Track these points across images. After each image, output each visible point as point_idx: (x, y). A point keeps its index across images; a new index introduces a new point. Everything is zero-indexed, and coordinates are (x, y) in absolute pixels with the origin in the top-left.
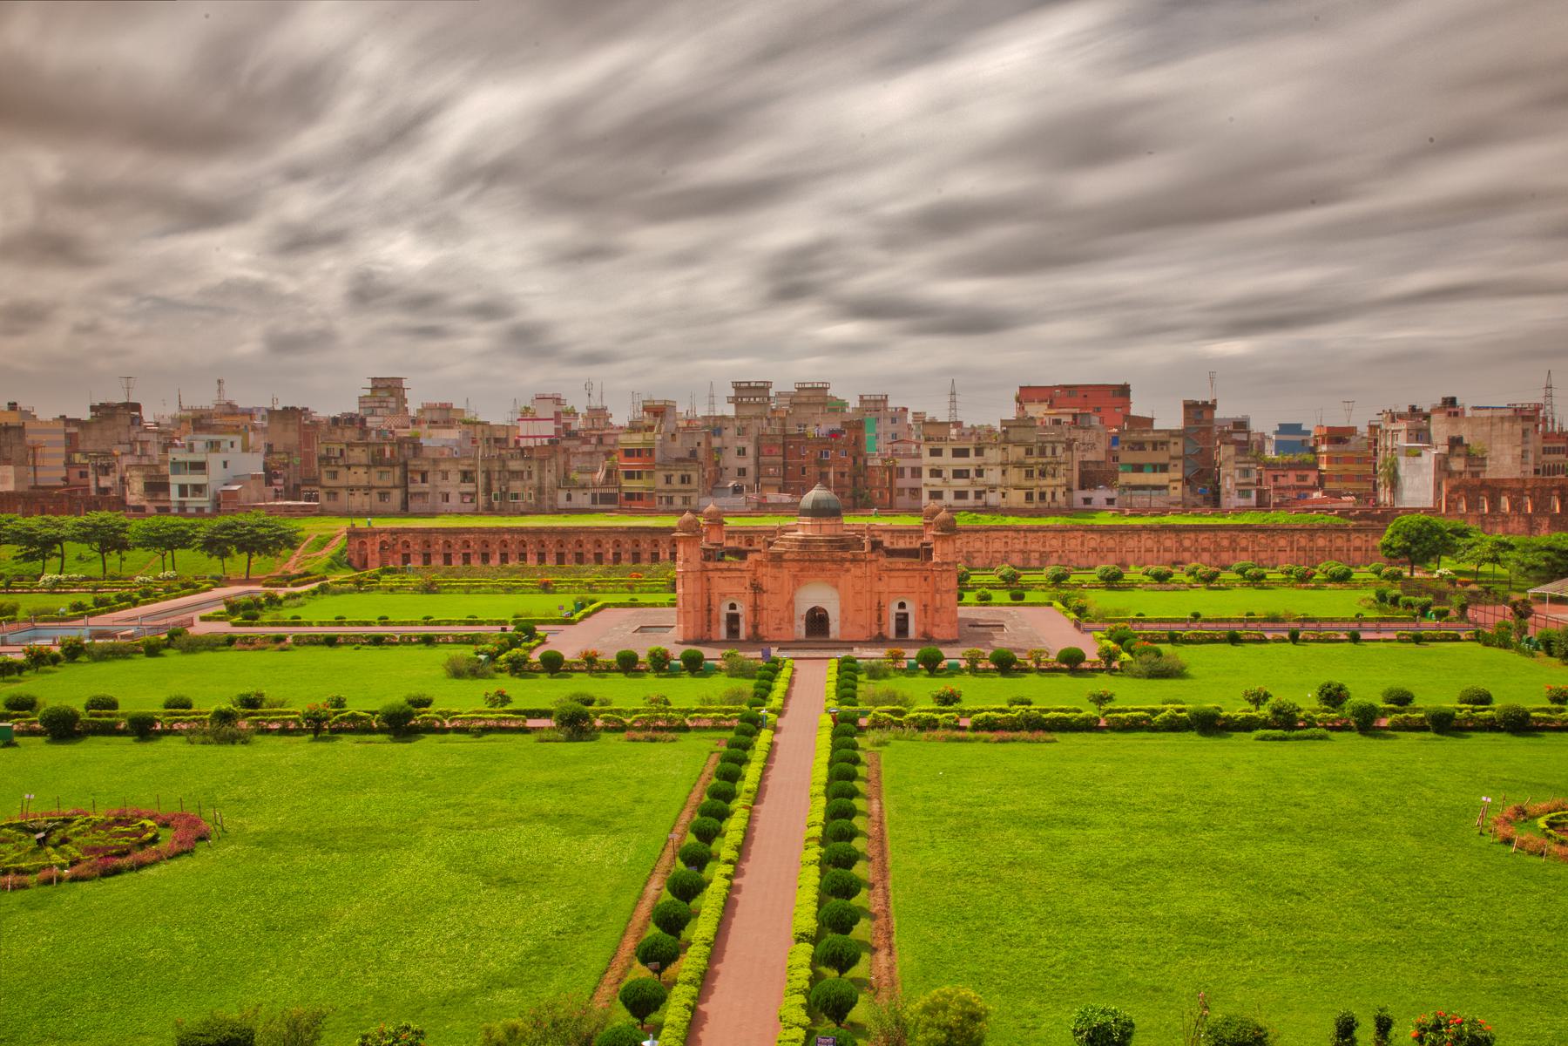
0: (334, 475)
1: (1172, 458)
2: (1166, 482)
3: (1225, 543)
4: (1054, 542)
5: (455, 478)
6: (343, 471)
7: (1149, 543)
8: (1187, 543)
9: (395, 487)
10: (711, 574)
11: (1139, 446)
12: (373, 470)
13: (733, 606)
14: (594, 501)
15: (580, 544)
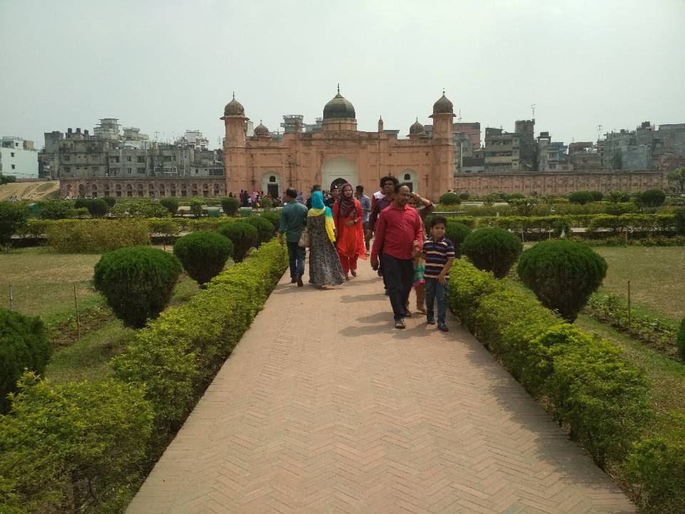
0: (68, 158)
1: (514, 148)
2: (511, 161)
3: (560, 182)
4: (464, 183)
5: (134, 160)
6: (72, 157)
7: (517, 183)
8: (539, 183)
9: (101, 165)
10: (253, 152)
11: (494, 142)
12: (89, 156)
13: (272, 179)
14: (211, 174)
15: (195, 186)
